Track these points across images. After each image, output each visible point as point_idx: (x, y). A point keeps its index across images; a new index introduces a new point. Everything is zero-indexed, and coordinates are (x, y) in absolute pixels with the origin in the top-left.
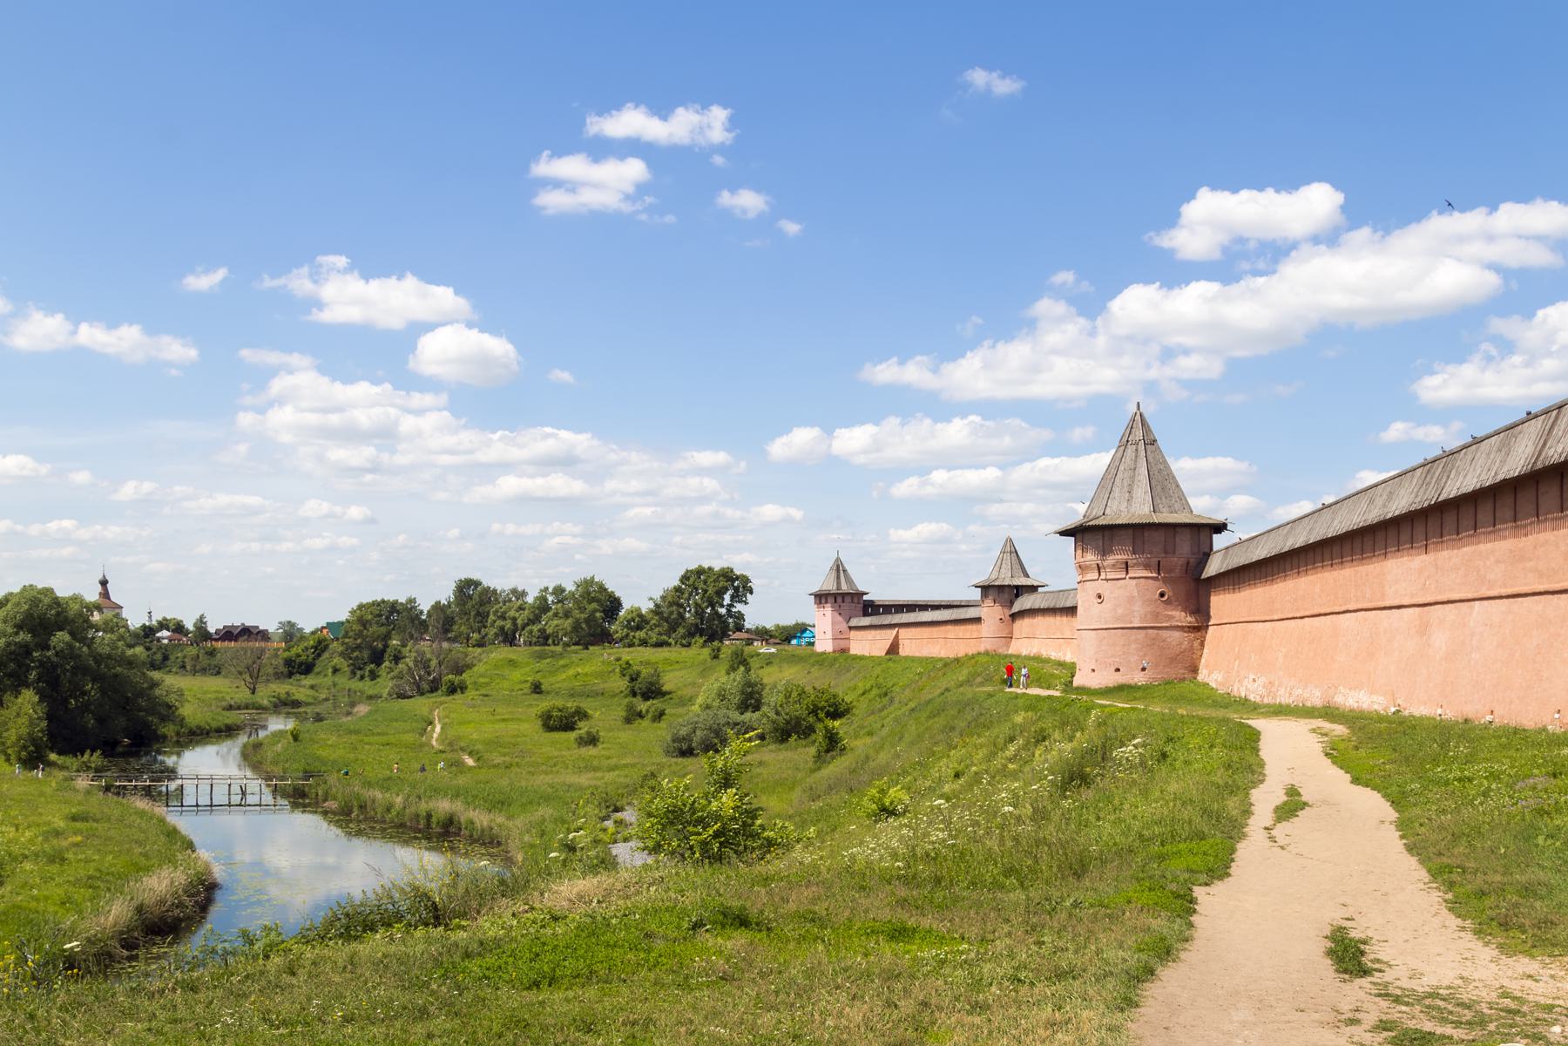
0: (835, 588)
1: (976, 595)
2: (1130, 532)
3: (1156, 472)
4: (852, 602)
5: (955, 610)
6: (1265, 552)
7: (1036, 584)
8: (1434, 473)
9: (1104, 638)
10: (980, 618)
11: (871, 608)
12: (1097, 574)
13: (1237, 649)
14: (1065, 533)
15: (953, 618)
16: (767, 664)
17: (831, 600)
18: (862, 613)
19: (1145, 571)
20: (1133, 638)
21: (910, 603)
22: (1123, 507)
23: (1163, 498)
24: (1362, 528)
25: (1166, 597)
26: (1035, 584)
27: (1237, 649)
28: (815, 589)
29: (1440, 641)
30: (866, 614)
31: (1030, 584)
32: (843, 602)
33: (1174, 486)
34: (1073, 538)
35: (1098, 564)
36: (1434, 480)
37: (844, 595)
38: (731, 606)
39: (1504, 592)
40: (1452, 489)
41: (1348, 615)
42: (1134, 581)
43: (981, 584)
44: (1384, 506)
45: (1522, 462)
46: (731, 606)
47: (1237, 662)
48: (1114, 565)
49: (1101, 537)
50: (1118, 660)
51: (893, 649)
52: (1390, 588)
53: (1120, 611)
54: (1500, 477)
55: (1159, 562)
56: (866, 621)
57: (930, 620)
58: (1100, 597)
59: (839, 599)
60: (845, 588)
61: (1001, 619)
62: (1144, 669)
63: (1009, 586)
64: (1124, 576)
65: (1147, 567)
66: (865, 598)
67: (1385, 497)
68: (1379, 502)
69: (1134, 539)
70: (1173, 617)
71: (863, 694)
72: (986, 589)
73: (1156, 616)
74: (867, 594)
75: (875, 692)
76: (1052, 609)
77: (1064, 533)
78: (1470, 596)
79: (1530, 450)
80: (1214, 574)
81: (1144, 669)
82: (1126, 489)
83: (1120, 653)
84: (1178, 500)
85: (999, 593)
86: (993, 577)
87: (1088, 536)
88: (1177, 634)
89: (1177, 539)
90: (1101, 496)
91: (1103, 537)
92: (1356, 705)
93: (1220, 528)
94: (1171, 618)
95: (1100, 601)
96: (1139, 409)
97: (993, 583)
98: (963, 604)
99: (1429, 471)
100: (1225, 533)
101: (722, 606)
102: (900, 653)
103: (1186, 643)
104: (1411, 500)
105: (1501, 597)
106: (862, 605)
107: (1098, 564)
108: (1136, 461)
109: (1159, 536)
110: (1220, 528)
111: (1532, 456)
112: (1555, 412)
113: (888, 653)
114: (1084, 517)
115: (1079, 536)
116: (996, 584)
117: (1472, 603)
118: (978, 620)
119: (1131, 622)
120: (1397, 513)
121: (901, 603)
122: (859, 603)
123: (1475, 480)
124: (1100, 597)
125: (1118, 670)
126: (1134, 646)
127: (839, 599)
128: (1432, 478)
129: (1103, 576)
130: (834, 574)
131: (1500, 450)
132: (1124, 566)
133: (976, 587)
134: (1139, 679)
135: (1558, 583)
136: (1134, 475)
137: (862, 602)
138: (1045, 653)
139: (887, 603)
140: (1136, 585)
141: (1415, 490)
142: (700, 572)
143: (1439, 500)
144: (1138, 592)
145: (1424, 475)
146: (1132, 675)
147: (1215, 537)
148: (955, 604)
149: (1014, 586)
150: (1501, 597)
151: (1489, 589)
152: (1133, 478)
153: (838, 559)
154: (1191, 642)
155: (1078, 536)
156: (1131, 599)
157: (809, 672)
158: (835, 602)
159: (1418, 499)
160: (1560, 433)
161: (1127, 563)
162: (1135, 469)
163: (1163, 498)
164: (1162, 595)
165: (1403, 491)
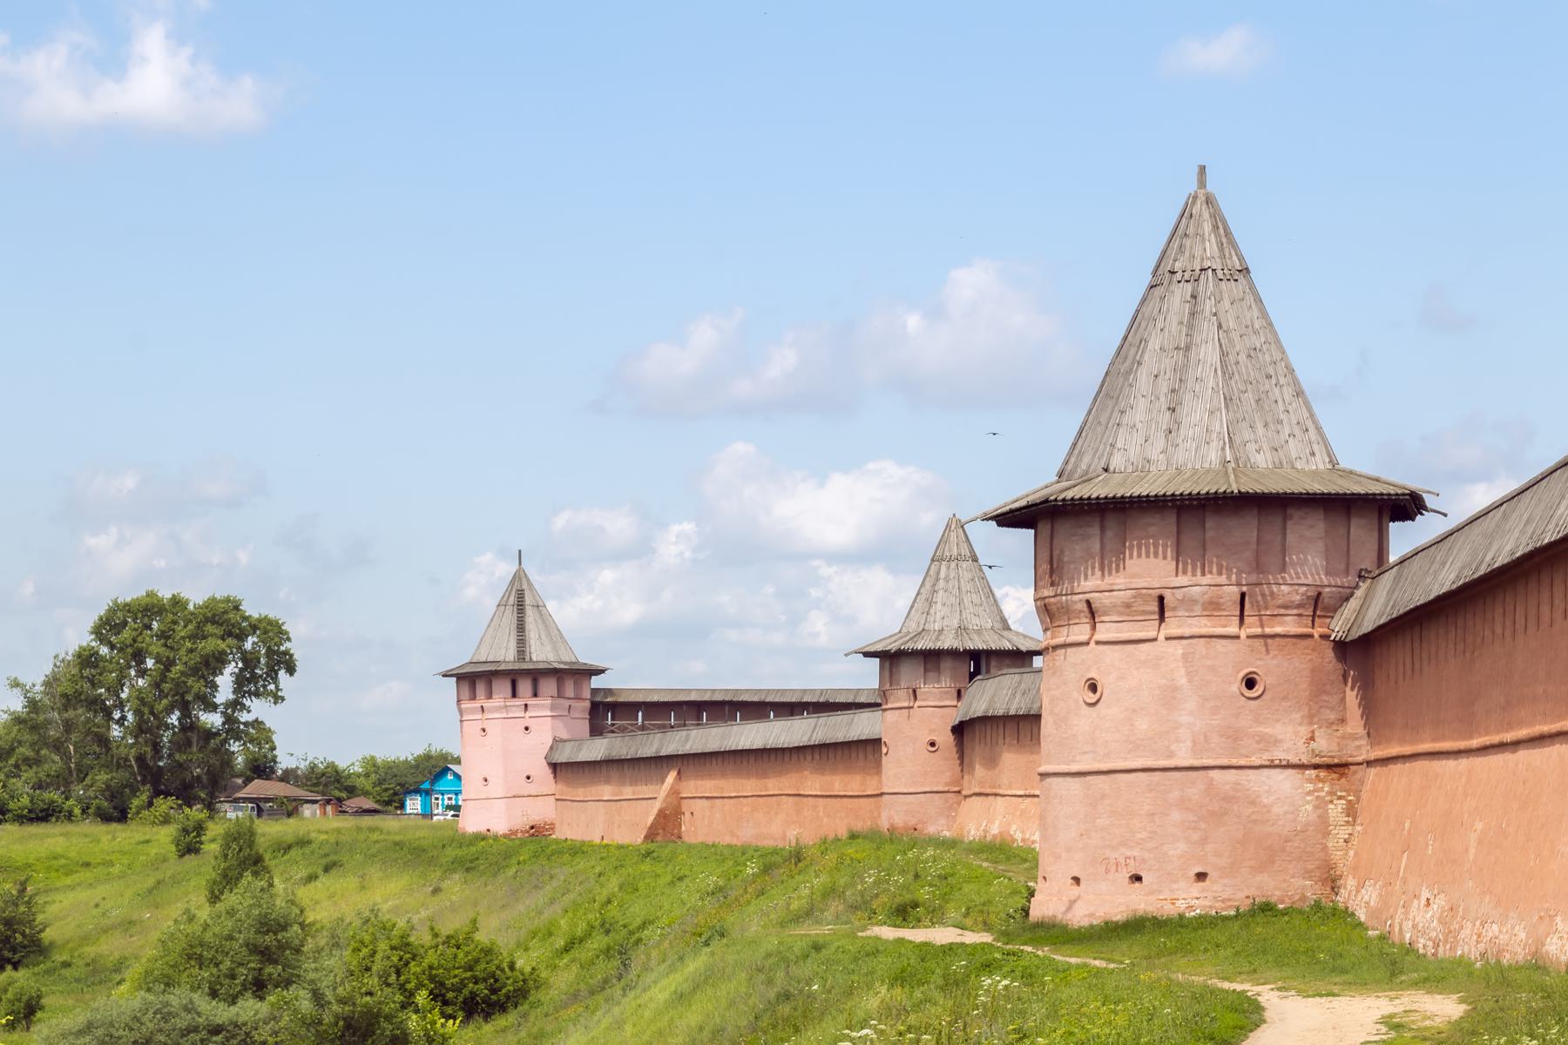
0: (511, 655)
1: (867, 676)
2: (1171, 519)
3: (1243, 358)
4: (560, 695)
7: (1025, 646)
9: (1103, 797)
10: (879, 740)
12: (1087, 628)
13: (1407, 825)
14: (1010, 519)
15: (819, 737)
16: (327, 869)
17: (503, 688)
18: (586, 725)
19: (1204, 621)
20: (1175, 795)
21: (718, 697)
22: (1155, 451)
23: (1259, 425)
26: (1024, 649)
27: (1407, 825)
28: (460, 658)
30: (596, 730)
31: (1008, 646)
32: (535, 695)
33: (1288, 392)
34: (1024, 538)
35: (1088, 603)
37: (537, 676)
38: (236, 704)
42: (1178, 648)
43: (879, 647)
46: (236, 704)
48: (1128, 606)
49: (1095, 530)
50: (1135, 853)
51: (666, 824)
53: (1143, 725)
55: (1243, 595)
57: (758, 744)
58: (1093, 688)
59: (525, 686)
60: (541, 653)
61: (933, 744)
62: (1201, 876)
63: (953, 654)
64: (1152, 634)
65: (1213, 607)
66: (596, 682)
69: (1178, 532)
70: (1277, 742)
71: (567, 949)
73: (1234, 736)
74: (602, 671)
75: (598, 942)
77: (1010, 519)
80: (1370, 629)
81: (1201, 876)
82: (1163, 403)
83: (1143, 835)
84: (1297, 432)
85: (926, 671)
86: (913, 627)
87: (1064, 528)
88: (1285, 782)
89: (1291, 538)
90: (1103, 420)
91: (1103, 529)
93: (1407, 506)
94: (1267, 742)
95: (1092, 698)
96: (1202, 183)
97: (910, 646)
98: (862, 699)
101: (213, 707)
102: (686, 838)
103: (1309, 807)
106: (587, 704)
107: (1088, 603)
108: (1190, 326)
109: (1245, 530)
110: (1407, 506)
113: (651, 836)
114: (1060, 475)
115: (1045, 527)
116: (919, 646)
118: (871, 747)
119: (1171, 755)
121: (693, 697)
122: (578, 698)
124: (1093, 688)
125: (1138, 878)
126: (1176, 816)
127: (525, 686)
129: (1104, 632)
130: (510, 618)
132: (1155, 607)
133: (867, 654)
134: (1189, 900)
136: (1185, 366)
137: (587, 694)
138: (1018, 836)
139: (655, 699)
140: (1185, 656)
142: (148, 609)
144: (1188, 673)
146: (1172, 891)
147: (1395, 528)
148: (841, 699)
149: (965, 650)
152: (1181, 372)
153: (519, 576)
154: (1321, 805)
155: (1040, 526)
156: (1169, 697)
157: (436, 891)
158: (514, 695)
161: (1161, 599)
162: (1188, 348)
163: (1259, 425)
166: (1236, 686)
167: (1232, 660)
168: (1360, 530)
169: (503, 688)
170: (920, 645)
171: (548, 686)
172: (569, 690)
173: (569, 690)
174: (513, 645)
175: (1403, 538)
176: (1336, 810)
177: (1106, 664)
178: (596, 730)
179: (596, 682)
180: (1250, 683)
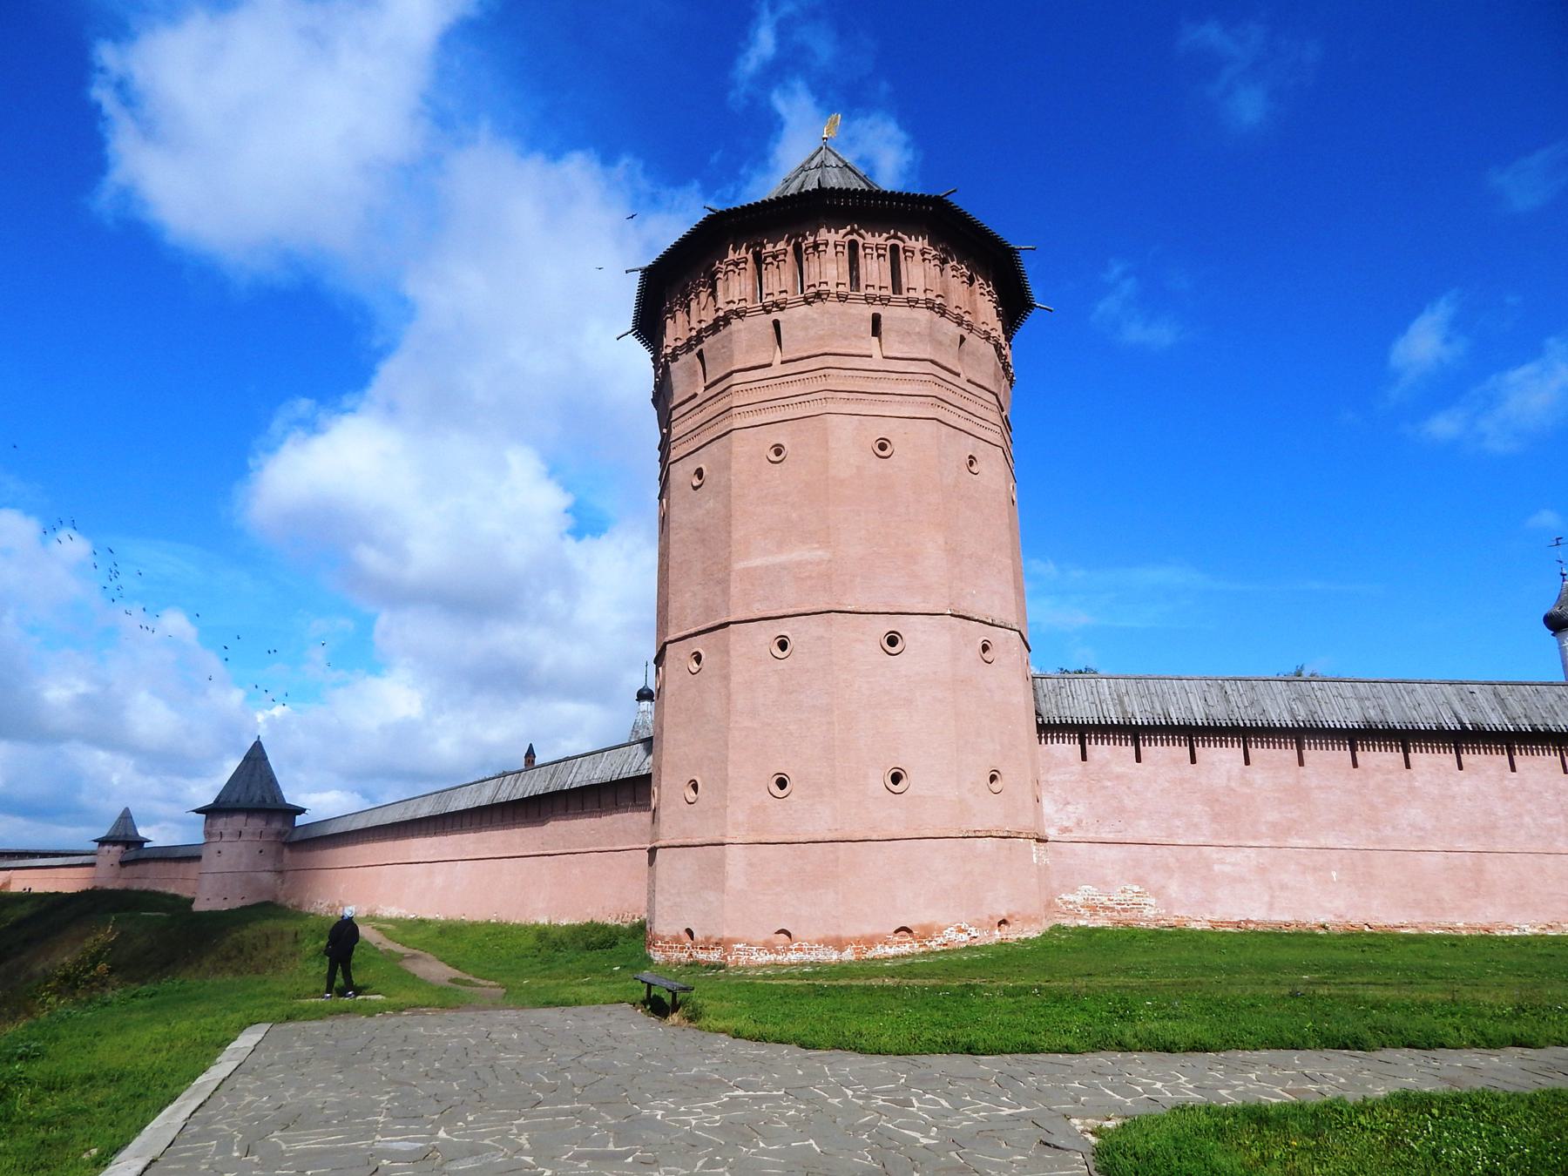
5: (76, 857)
14: (198, 811)
24: (402, 822)
29: (439, 881)
34: (204, 815)
40: (452, 808)
44: (415, 811)
65: (254, 834)
67: (415, 806)
68: (412, 809)
72: (102, 842)
79: (491, 794)
81: (243, 898)
86: (111, 834)
88: (266, 875)
92: (389, 915)
93: (302, 811)
100: (303, 814)
131: (476, 792)
147: (297, 817)
151: (467, 855)
164: (261, 852)
165: (425, 805)
166: (257, 852)
170: (113, 839)
176: (279, 882)
177: (223, 846)
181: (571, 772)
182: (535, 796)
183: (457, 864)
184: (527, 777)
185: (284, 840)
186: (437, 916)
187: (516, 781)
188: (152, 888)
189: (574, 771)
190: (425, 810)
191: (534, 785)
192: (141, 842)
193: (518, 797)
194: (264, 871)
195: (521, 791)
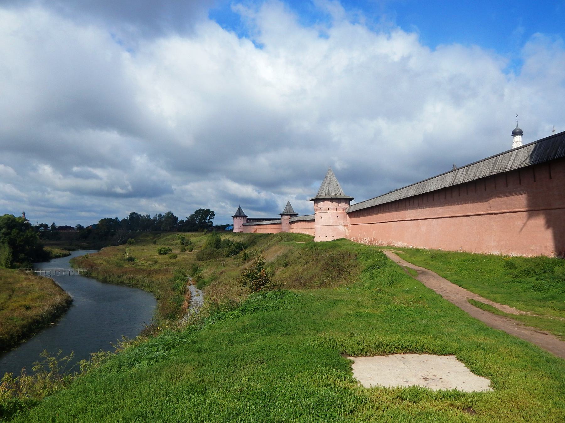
1: (280, 216)
6: (368, 206)
8: (421, 186)
11: (249, 220)
13: (359, 231)
25: (338, 217)
27: (359, 231)
36: (421, 188)
38: (209, 220)
39: (442, 216)
41: (394, 222)
44: (406, 194)
45: (449, 183)
46: (209, 220)
47: (359, 235)
52: (407, 215)
54: (442, 187)
56: (248, 224)
59: (240, 218)
63: (289, 214)
65: (334, 209)
66: (247, 217)
76: (312, 220)
78: (432, 217)
99: (419, 185)
101: (207, 220)
104: (414, 193)
105: (442, 218)
111: (451, 182)
112: (457, 171)
117: (433, 219)
120: (410, 196)
123: (434, 188)
127: (240, 218)
128: (420, 187)
129: (322, 212)
131: (441, 180)
135: (458, 214)
140: (331, 214)
141: (415, 190)
143: (424, 192)
145: (417, 186)
150: (442, 218)
154: (345, 229)
159: (417, 192)
160: (460, 176)
167: (336, 214)
168: (348, 201)
169: (238, 218)
171: (242, 218)
172: (244, 218)
173: (244, 218)
174: (239, 214)
175: (352, 203)
176: (347, 230)
178: (247, 222)
179: (247, 217)
180: (338, 217)
181: (510, 160)
182: (483, 178)
183: (433, 220)
184: (475, 168)
185: (346, 211)
186: (425, 247)
187: (467, 171)
188: (301, 232)
189: (512, 158)
190: (411, 193)
191: (481, 172)
192: (295, 215)
193: (470, 180)
194: (340, 225)
195: (472, 176)
